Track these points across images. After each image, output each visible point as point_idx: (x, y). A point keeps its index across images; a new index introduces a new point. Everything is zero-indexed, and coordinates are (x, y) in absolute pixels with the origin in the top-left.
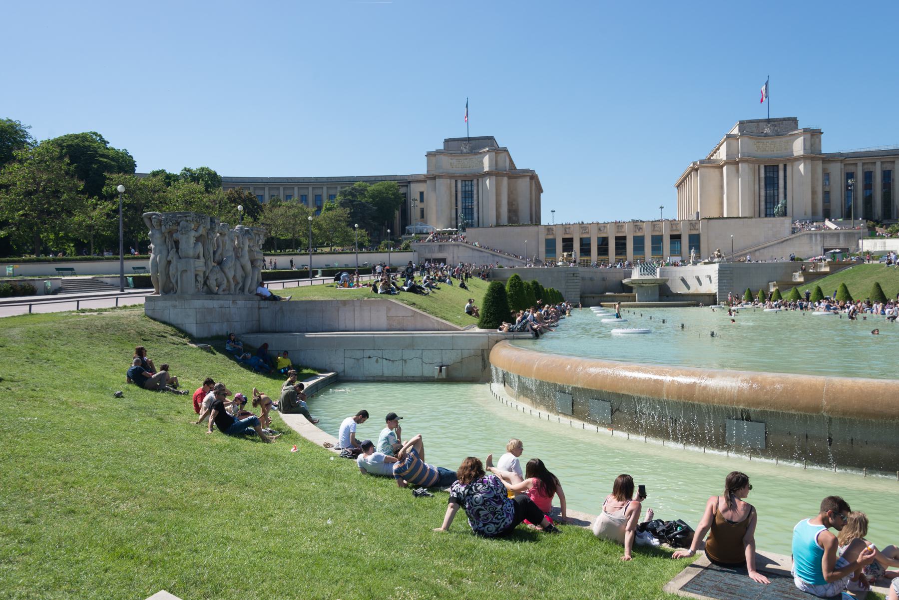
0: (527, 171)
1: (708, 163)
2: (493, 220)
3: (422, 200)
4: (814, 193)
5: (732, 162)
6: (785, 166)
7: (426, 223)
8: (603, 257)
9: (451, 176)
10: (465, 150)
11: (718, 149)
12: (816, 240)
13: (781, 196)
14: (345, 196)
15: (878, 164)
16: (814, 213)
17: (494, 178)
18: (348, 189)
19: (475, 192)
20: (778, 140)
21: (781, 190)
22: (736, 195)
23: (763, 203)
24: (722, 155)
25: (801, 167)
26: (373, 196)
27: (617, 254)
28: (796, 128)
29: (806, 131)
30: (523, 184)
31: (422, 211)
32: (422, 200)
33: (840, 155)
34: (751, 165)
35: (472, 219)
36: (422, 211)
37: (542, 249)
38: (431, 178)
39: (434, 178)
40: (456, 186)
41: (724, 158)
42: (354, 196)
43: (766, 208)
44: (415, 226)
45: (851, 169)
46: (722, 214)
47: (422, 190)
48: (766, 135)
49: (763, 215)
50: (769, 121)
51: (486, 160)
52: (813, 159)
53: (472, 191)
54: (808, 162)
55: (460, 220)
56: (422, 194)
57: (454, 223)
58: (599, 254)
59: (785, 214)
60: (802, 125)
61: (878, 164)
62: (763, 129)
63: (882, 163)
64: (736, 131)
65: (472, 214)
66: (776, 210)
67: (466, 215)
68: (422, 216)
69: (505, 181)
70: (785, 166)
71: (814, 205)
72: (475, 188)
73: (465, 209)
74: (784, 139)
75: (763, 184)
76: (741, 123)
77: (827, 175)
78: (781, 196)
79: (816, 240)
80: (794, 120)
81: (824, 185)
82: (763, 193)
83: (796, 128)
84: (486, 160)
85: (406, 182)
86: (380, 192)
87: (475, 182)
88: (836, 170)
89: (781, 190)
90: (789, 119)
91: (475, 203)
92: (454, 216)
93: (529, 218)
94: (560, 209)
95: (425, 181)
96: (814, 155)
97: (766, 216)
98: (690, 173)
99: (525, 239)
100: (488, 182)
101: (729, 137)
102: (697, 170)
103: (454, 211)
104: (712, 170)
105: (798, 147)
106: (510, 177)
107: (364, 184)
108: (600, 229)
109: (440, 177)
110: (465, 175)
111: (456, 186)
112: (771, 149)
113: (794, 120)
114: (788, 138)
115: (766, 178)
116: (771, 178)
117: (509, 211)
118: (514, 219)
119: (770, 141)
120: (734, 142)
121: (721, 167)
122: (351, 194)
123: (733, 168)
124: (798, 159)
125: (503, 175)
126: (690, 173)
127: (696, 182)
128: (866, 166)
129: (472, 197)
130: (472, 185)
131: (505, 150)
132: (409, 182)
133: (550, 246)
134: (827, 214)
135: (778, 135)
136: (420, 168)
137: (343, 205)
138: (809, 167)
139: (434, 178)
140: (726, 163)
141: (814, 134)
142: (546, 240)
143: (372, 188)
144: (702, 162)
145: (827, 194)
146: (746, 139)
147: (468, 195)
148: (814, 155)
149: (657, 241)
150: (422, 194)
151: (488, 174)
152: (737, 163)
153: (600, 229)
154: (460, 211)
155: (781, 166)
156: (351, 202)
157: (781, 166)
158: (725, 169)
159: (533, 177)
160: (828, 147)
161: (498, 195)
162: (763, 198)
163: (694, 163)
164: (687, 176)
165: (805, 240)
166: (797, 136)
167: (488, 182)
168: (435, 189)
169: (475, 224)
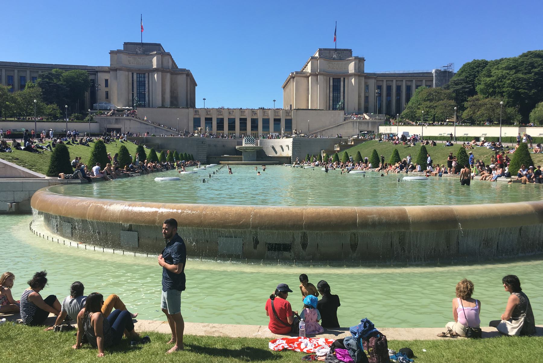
0: (183, 70)
1: (301, 74)
2: (159, 103)
3: (107, 85)
4: (359, 97)
5: (314, 74)
6: (344, 79)
7: (110, 102)
8: (231, 132)
9: (129, 70)
10: (139, 52)
11: (307, 65)
12: (356, 125)
13: (342, 97)
14: (43, 78)
15: (394, 81)
16: (359, 109)
17: (160, 73)
18: (46, 73)
19: (147, 82)
20: (340, 63)
21: (342, 94)
22: (315, 96)
23: (331, 102)
24: (309, 69)
25: (353, 80)
26: (67, 80)
27: (241, 130)
28: (351, 56)
29: (356, 58)
30: (181, 80)
31: (107, 93)
32: (107, 85)
33: (375, 74)
34: (325, 77)
35: (145, 101)
36: (107, 93)
37: (191, 124)
38: (112, 70)
39: (116, 70)
40: (133, 77)
41: (310, 72)
42: (50, 79)
43: (333, 105)
44: (101, 103)
45: (380, 83)
46: (308, 107)
47: (107, 78)
48: (334, 59)
49: (331, 109)
50: (336, 50)
51: (155, 60)
52: (359, 76)
53: (144, 81)
54: (357, 77)
55: (135, 102)
56: (107, 81)
57: (131, 103)
58: (229, 130)
59: (343, 109)
60: (354, 55)
61: (394, 81)
62: (333, 55)
63: (397, 81)
64: (317, 55)
65: (145, 98)
66: (338, 106)
67: (140, 97)
68: (107, 97)
69: (168, 76)
70: (344, 79)
71: (359, 104)
72: (147, 80)
73: (140, 94)
74: (344, 62)
75: (331, 89)
76: (320, 50)
77: (367, 87)
78: (342, 97)
79: (356, 125)
80: (350, 51)
81: (365, 92)
82: (331, 95)
83: (351, 56)
84: (155, 60)
85: (95, 71)
86: (73, 78)
87: (147, 74)
88: (372, 83)
89: (342, 94)
90: (347, 50)
91: (147, 90)
92: (131, 98)
93: (185, 103)
94: (210, 97)
95: (109, 72)
96: (360, 73)
97: (333, 109)
98: (290, 80)
99: (181, 117)
100: (156, 76)
101: (313, 58)
102: (294, 78)
103: (131, 95)
104: (303, 78)
105: (351, 68)
106: (172, 74)
107: (60, 70)
108: (230, 113)
109: (120, 70)
110: (139, 70)
111: (133, 77)
112: (335, 67)
113: (350, 51)
114: (346, 62)
115: (333, 85)
116: (336, 85)
117: (172, 97)
118: (174, 103)
119: (336, 63)
120: (315, 61)
121: (308, 77)
122: (47, 77)
123: (315, 78)
124: (351, 75)
125: (167, 72)
126: (290, 80)
127: (293, 85)
128: (388, 82)
129: (145, 86)
130: (144, 77)
131: (169, 54)
132: (97, 72)
133: (197, 123)
134: (367, 111)
135: (340, 59)
136: (105, 62)
137: (40, 85)
138: (357, 80)
139: (116, 70)
140: (311, 75)
141: (360, 61)
142: (194, 118)
143: (65, 74)
144: (297, 73)
145: (367, 98)
146: (322, 60)
147: (141, 84)
148: (360, 73)
149: (266, 122)
150: (107, 81)
151: (156, 70)
152: (317, 75)
153: (230, 113)
154: (135, 95)
155: (342, 79)
156: (48, 83)
157: (342, 79)
158: (310, 78)
159: (188, 74)
160: (368, 69)
161: (163, 85)
162: (331, 98)
163: (292, 73)
164: (289, 81)
165: (351, 125)
166: (351, 61)
167: (156, 76)
168: (116, 78)
169: (147, 105)
